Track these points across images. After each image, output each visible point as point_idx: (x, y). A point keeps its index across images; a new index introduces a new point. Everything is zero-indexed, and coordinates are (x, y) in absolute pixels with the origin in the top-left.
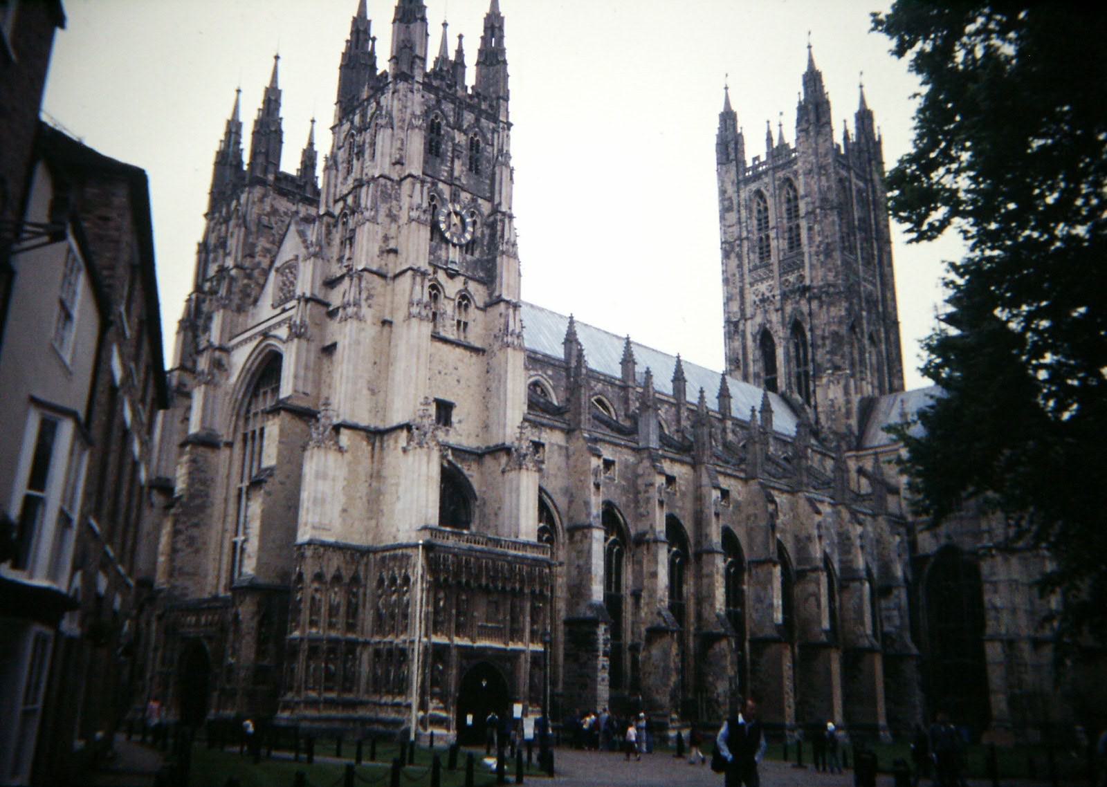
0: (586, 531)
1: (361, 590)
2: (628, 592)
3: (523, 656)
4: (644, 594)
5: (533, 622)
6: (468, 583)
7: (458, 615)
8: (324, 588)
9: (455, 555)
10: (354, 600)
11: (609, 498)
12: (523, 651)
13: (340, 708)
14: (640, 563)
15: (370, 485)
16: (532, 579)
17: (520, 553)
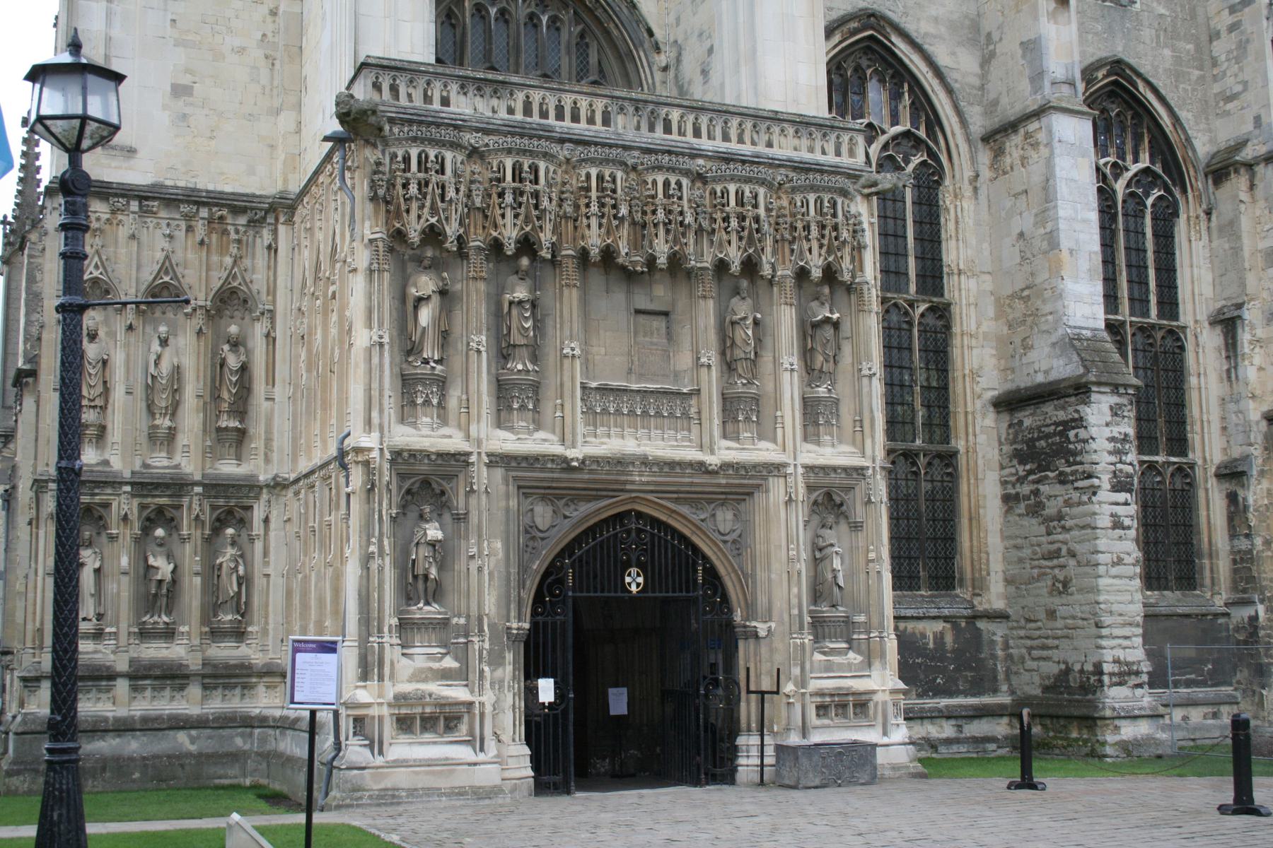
0: (1033, 126)
1: (259, 329)
2: (1203, 316)
3: (777, 490)
4: (1251, 314)
5: (811, 373)
6: (527, 245)
7: (504, 353)
8: (119, 324)
9: (474, 153)
10: (233, 362)
11: (1119, 49)
12: (776, 469)
13: (195, 690)
14: (1231, 229)
15: (274, 13)
16: (789, 234)
17: (746, 149)
